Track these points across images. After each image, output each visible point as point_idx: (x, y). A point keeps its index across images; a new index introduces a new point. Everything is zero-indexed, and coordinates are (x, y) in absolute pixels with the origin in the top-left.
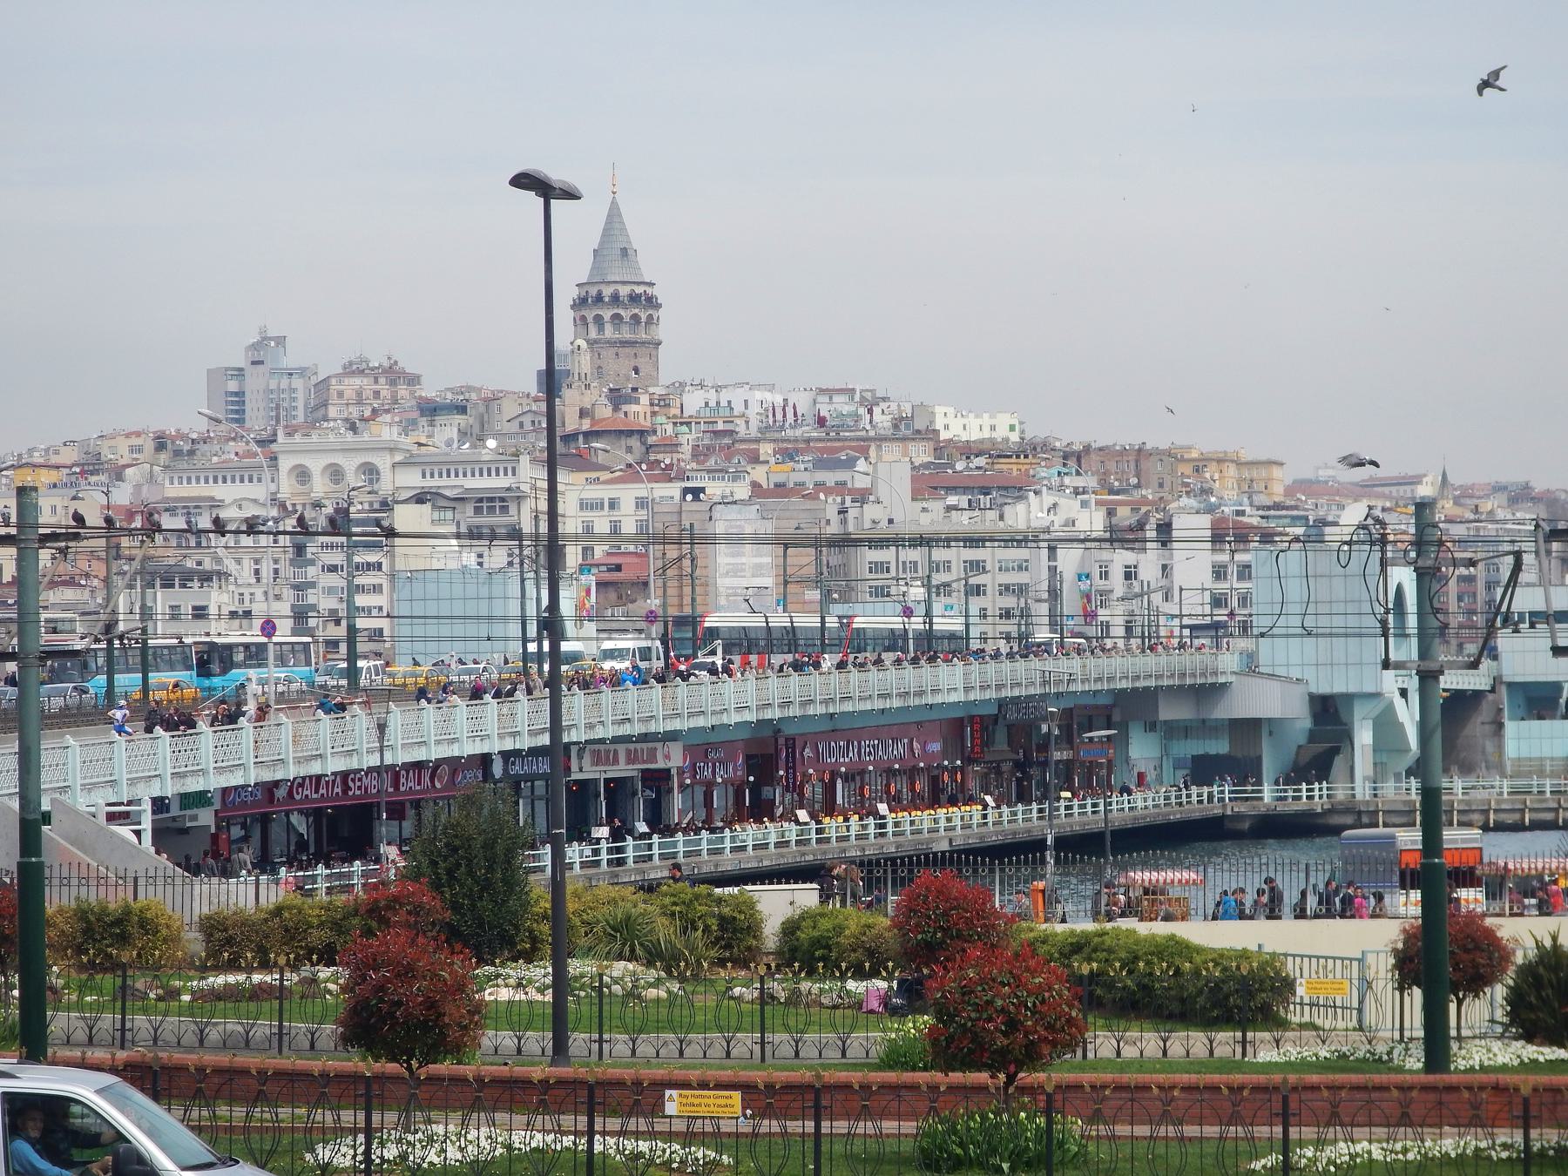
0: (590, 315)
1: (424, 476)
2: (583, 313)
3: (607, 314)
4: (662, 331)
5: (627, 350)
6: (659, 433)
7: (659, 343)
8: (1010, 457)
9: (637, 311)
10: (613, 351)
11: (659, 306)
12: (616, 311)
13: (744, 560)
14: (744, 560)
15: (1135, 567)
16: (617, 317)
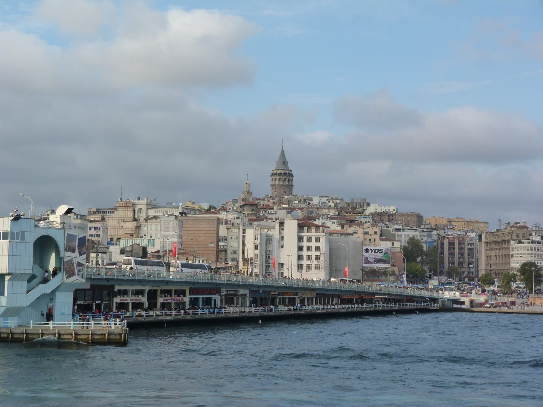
0: (274, 178)
1: (155, 212)
2: (273, 177)
3: (278, 178)
4: (294, 183)
5: (283, 187)
6: (262, 206)
7: (293, 186)
8: (358, 213)
9: (285, 177)
10: (279, 187)
11: (294, 176)
12: (280, 177)
13: (169, 233)
14: (169, 233)
15: (272, 236)
16: (280, 179)
